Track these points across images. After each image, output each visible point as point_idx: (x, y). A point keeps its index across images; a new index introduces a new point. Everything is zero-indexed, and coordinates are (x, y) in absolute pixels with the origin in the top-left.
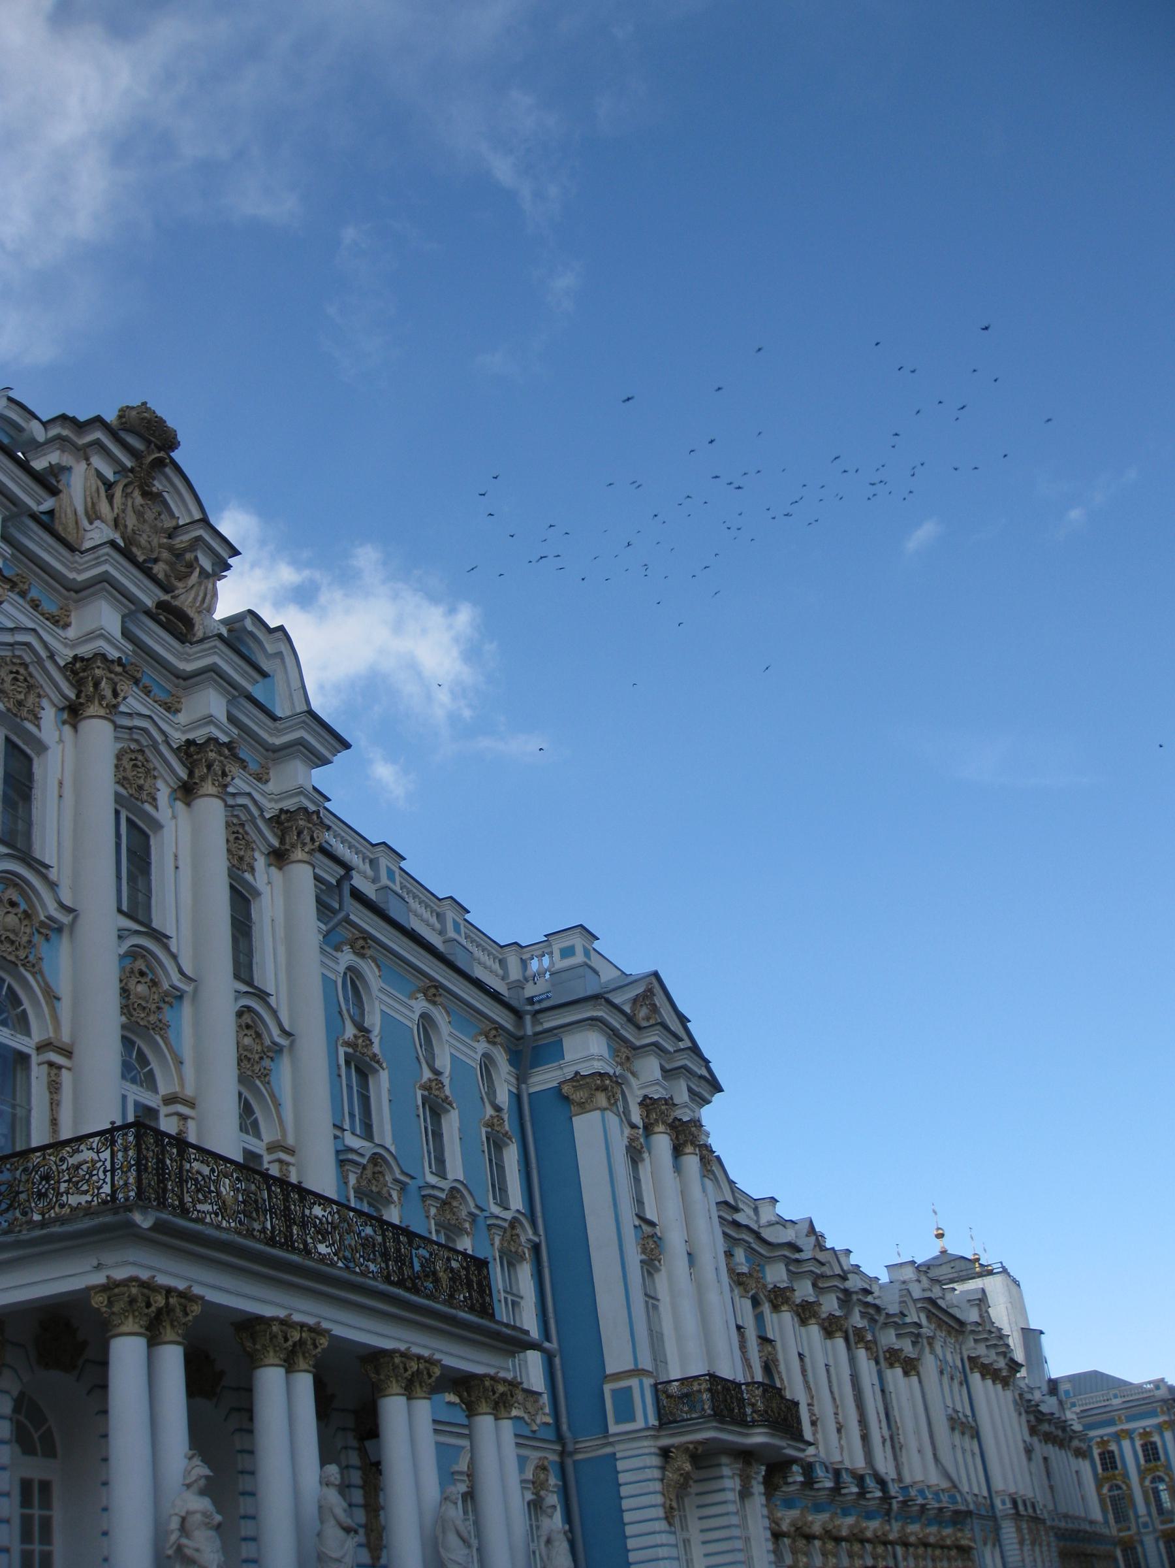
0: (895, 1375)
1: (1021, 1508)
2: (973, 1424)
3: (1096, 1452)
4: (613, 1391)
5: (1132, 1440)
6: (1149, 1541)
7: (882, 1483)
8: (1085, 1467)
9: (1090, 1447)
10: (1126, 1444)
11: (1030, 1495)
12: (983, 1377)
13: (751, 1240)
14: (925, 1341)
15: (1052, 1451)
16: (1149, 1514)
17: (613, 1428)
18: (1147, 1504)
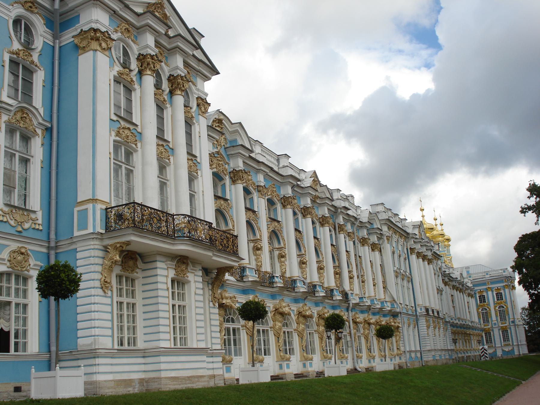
0: (365, 251)
1: (431, 313)
2: (409, 276)
3: (478, 295)
4: (78, 211)
5: (492, 291)
6: (496, 331)
7: (345, 295)
8: (472, 302)
9: (475, 293)
10: (490, 293)
11: (438, 308)
12: (418, 257)
13: (268, 171)
14: (385, 238)
15: (455, 293)
16: (497, 320)
17: (76, 233)
18: (496, 316)
